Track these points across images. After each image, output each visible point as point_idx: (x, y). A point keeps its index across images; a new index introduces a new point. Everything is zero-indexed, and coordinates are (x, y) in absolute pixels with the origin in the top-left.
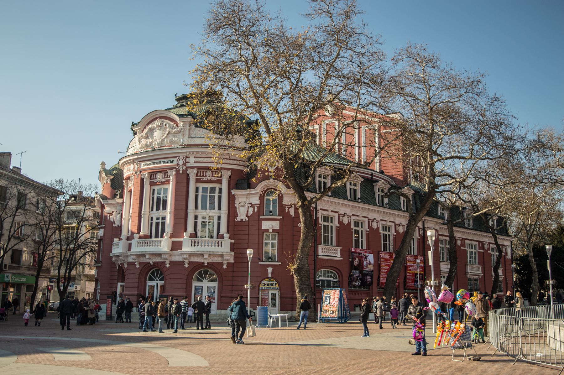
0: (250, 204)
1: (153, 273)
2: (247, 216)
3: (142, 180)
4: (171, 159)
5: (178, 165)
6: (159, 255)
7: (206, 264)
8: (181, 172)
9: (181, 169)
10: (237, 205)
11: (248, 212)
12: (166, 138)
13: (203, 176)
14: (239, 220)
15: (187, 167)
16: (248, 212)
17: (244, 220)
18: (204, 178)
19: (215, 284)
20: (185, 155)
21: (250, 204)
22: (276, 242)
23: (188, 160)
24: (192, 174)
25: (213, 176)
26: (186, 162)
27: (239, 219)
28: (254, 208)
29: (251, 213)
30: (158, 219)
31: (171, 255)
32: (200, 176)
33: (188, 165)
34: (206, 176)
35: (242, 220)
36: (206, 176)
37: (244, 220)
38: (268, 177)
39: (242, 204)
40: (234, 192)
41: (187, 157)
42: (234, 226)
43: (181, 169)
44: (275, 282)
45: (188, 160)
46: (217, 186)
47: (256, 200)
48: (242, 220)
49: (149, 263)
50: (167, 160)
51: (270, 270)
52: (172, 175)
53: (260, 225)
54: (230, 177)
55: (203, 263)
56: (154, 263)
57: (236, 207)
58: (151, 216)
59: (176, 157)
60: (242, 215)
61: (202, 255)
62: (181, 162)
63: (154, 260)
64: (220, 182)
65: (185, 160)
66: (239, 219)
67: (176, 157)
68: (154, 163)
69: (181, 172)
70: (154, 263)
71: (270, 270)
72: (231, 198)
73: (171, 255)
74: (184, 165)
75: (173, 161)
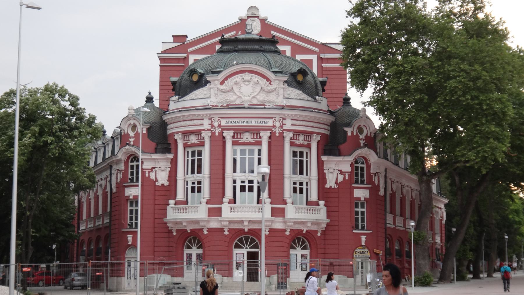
0: (339, 170)
1: (241, 240)
2: (336, 182)
3: (224, 138)
4: (266, 120)
5: (274, 126)
6: (197, 222)
7: (304, 232)
8: (277, 134)
9: (277, 131)
10: (326, 171)
11: (337, 179)
12: (257, 95)
13: (296, 139)
14: (328, 187)
15: (284, 130)
16: (337, 179)
17: (333, 187)
18: (298, 142)
19: (307, 252)
20: (282, 116)
21: (339, 170)
22: (365, 210)
23: (284, 122)
24: (288, 136)
25: (304, 140)
26: (283, 124)
27: (328, 186)
28: (345, 175)
29: (342, 180)
30: (243, 182)
31: (272, 222)
32: (294, 139)
33: (285, 127)
34: (299, 140)
35: (331, 187)
36: (299, 140)
37: (333, 187)
38: (358, 147)
39: (331, 170)
40: (324, 158)
41: (283, 119)
42: (324, 192)
43: (277, 131)
44: (366, 250)
45: (284, 122)
46: (305, 150)
47: (347, 168)
48: (331, 187)
49: (244, 230)
50: (259, 120)
51: (363, 238)
52: (265, 136)
53: (352, 193)
54: (319, 141)
55: (303, 231)
56: (249, 230)
57: (325, 174)
58: (235, 178)
59: (272, 118)
60: (331, 183)
61: (242, 222)
62: (278, 124)
63: (251, 227)
64: (309, 146)
65: (282, 122)
66: (328, 186)
67: (272, 118)
68: (243, 122)
69: (277, 134)
70: (249, 230)
71: (363, 238)
72: (320, 165)
73: (208, 222)
74: (281, 127)
75: (267, 122)
